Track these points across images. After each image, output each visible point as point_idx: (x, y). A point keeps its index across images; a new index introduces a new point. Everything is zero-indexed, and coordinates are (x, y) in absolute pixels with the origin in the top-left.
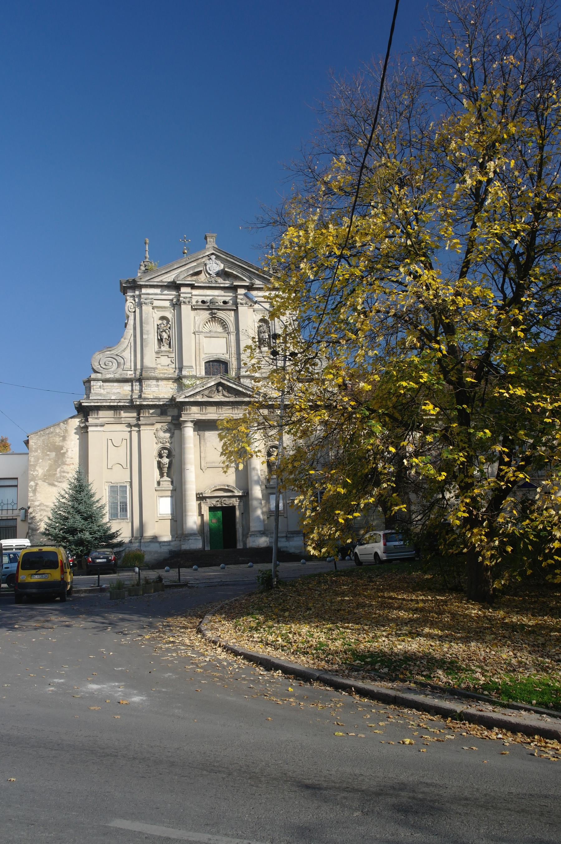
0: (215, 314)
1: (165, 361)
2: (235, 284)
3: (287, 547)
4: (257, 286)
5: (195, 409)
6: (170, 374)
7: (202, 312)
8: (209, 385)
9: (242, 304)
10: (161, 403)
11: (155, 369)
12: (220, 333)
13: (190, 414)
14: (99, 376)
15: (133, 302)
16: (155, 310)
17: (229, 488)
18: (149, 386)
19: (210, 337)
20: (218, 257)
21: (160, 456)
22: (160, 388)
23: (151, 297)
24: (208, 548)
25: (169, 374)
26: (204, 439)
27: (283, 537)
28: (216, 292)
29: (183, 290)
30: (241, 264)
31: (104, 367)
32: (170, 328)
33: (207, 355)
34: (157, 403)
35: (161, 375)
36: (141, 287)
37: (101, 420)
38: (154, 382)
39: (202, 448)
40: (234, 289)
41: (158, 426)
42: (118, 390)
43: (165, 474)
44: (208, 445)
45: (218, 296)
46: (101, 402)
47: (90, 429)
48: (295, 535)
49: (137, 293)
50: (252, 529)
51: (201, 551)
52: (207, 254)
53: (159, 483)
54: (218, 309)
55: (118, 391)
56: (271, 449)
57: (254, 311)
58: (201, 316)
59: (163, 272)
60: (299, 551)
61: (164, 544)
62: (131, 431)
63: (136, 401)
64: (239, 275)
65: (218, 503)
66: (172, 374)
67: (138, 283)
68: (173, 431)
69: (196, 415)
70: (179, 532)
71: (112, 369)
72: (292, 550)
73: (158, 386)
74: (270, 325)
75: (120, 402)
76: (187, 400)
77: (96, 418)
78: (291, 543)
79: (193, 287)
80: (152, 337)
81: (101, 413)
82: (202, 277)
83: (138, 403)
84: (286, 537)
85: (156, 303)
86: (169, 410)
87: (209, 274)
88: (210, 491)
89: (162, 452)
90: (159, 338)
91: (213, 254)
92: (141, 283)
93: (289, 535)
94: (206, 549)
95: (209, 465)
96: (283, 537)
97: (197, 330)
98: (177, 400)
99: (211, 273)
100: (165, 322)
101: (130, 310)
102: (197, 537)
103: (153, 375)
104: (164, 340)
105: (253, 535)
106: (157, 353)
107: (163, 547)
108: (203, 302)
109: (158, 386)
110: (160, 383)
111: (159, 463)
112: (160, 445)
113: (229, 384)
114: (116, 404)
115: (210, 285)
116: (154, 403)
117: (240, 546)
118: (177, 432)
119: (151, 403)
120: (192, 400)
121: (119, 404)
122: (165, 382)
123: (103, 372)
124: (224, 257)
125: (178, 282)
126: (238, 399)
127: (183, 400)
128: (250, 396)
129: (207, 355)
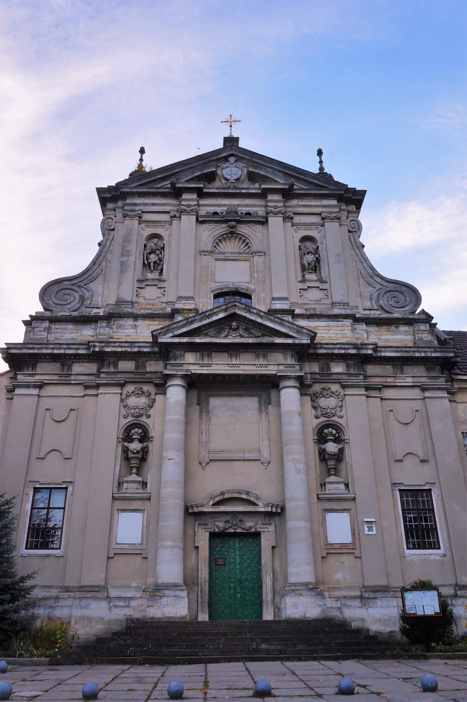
0: (232, 227)
1: (151, 293)
2: (263, 186)
3: (363, 620)
4: (297, 192)
5: (190, 358)
6: (156, 310)
7: (212, 226)
8: (215, 318)
9: (274, 213)
10: (136, 350)
11: (132, 303)
12: (240, 253)
13: (182, 365)
14: (48, 314)
15: (114, 218)
16: (143, 225)
17: (249, 498)
18: (119, 327)
19: (225, 260)
20: (239, 159)
21: (128, 438)
22: (139, 330)
23: (138, 208)
24: (204, 617)
25: (154, 310)
26: (208, 412)
27: (354, 598)
28: (235, 202)
29: (184, 196)
30: (272, 166)
31: (57, 302)
32: (163, 248)
33: (218, 284)
34: (129, 350)
35: (143, 312)
36: (124, 196)
37: (37, 377)
38: (130, 322)
39: (204, 426)
40: (263, 194)
41: (130, 388)
42: (72, 335)
43: (134, 470)
44: (213, 422)
45: (238, 206)
46: (39, 349)
47: (18, 391)
48: (378, 595)
49: (120, 204)
50: (292, 579)
51: (185, 623)
52: (224, 154)
53: (120, 484)
54: (239, 222)
55: (73, 335)
56: (326, 431)
57: (293, 226)
58: (211, 232)
59: (159, 176)
60: (388, 629)
61: (117, 604)
62: (84, 396)
63: (95, 346)
64: (270, 176)
65: (230, 525)
66: (162, 309)
67: (121, 190)
68: (153, 397)
69: (191, 367)
70: (150, 581)
71: (70, 306)
72: (374, 628)
73: (135, 327)
74: (318, 244)
75: (69, 349)
76: (176, 340)
77: (30, 375)
78: (371, 611)
79: (201, 194)
80: (135, 260)
81: (42, 367)
82: (217, 184)
83: (97, 349)
84: (361, 597)
85: (147, 217)
86: (149, 362)
87: (227, 180)
88: (211, 502)
89: (133, 431)
90: (146, 262)
91: (232, 155)
92: (126, 190)
93: (366, 595)
94: (200, 619)
95: (213, 456)
96: (354, 598)
97: (203, 248)
98: (160, 340)
99: (228, 177)
100: (155, 240)
101: (108, 227)
102: (179, 593)
103: (130, 310)
104: (152, 264)
105: (293, 591)
106: (139, 281)
107: (114, 610)
108: (215, 213)
109: (135, 327)
110: (140, 323)
111: (126, 450)
112: (130, 419)
113: (248, 316)
114: (62, 351)
115: (226, 191)
116: (124, 349)
117: (268, 616)
118: (159, 398)
119: (119, 349)
120: (185, 340)
121: (68, 352)
122: (147, 322)
123: (54, 309)
124: (248, 157)
125: (178, 185)
126: (266, 340)
127: (169, 340)
128: (287, 336)
129: (218, 284)
